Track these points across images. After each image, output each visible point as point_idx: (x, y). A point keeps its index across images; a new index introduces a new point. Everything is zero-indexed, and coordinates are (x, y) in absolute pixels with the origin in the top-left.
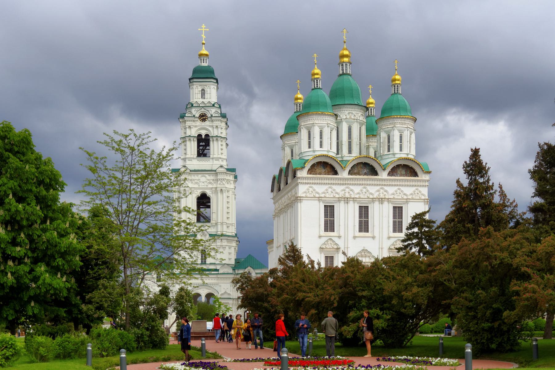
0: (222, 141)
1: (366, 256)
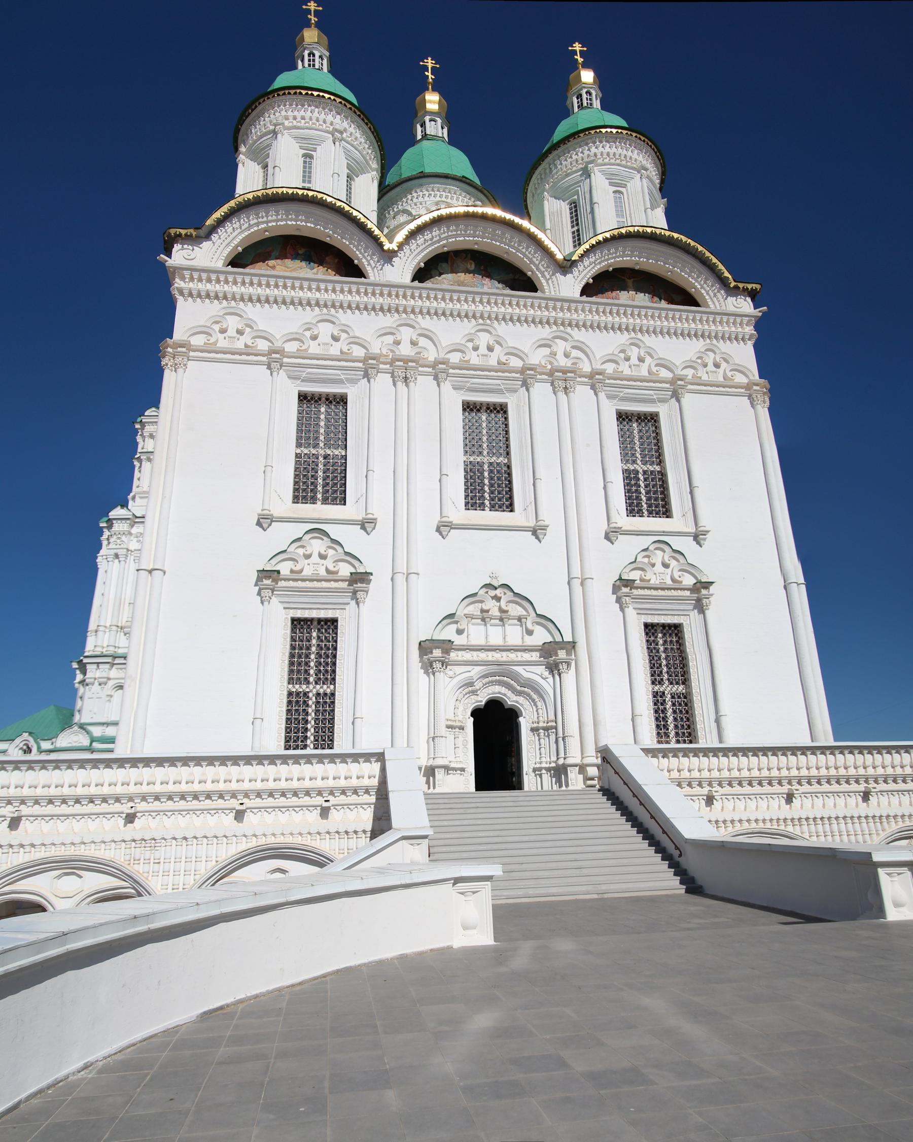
1: (503, 617)
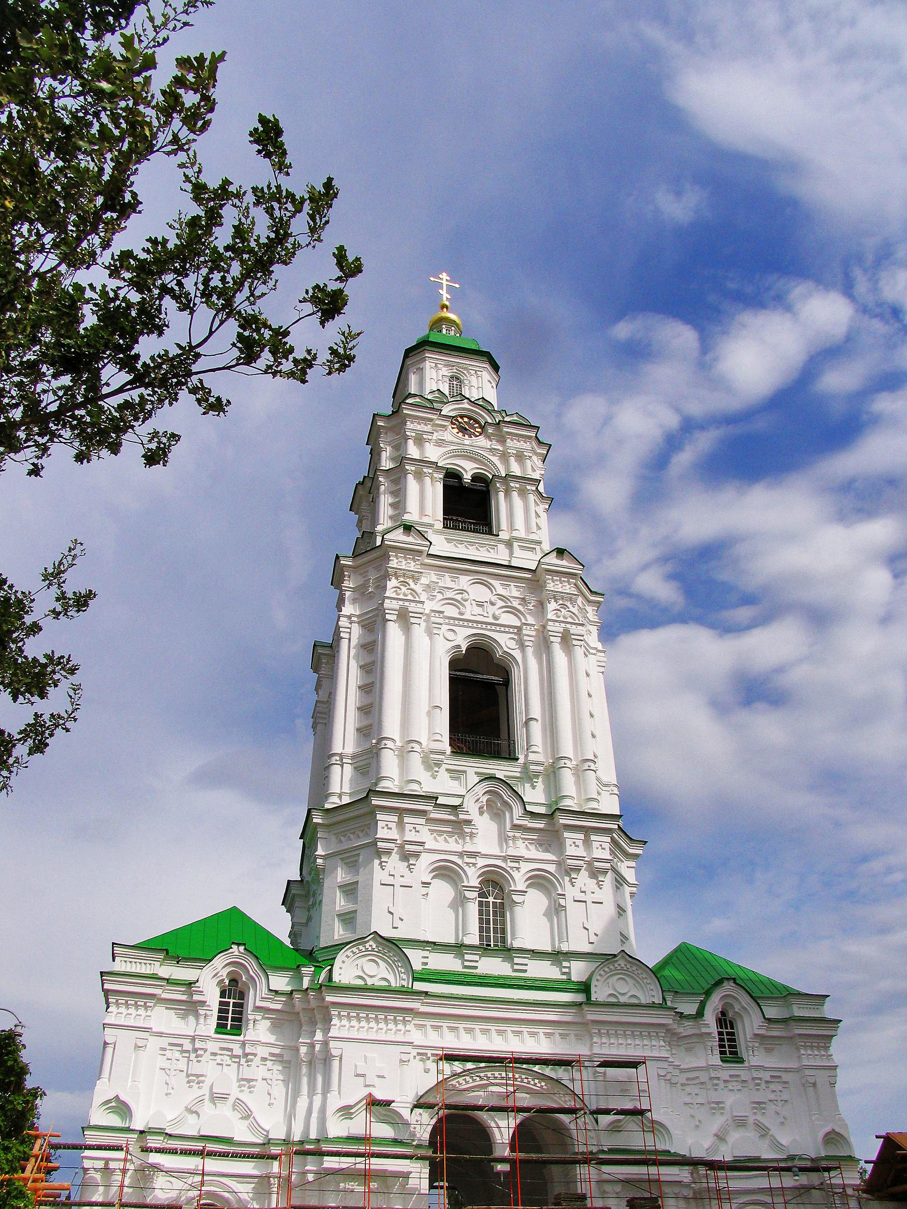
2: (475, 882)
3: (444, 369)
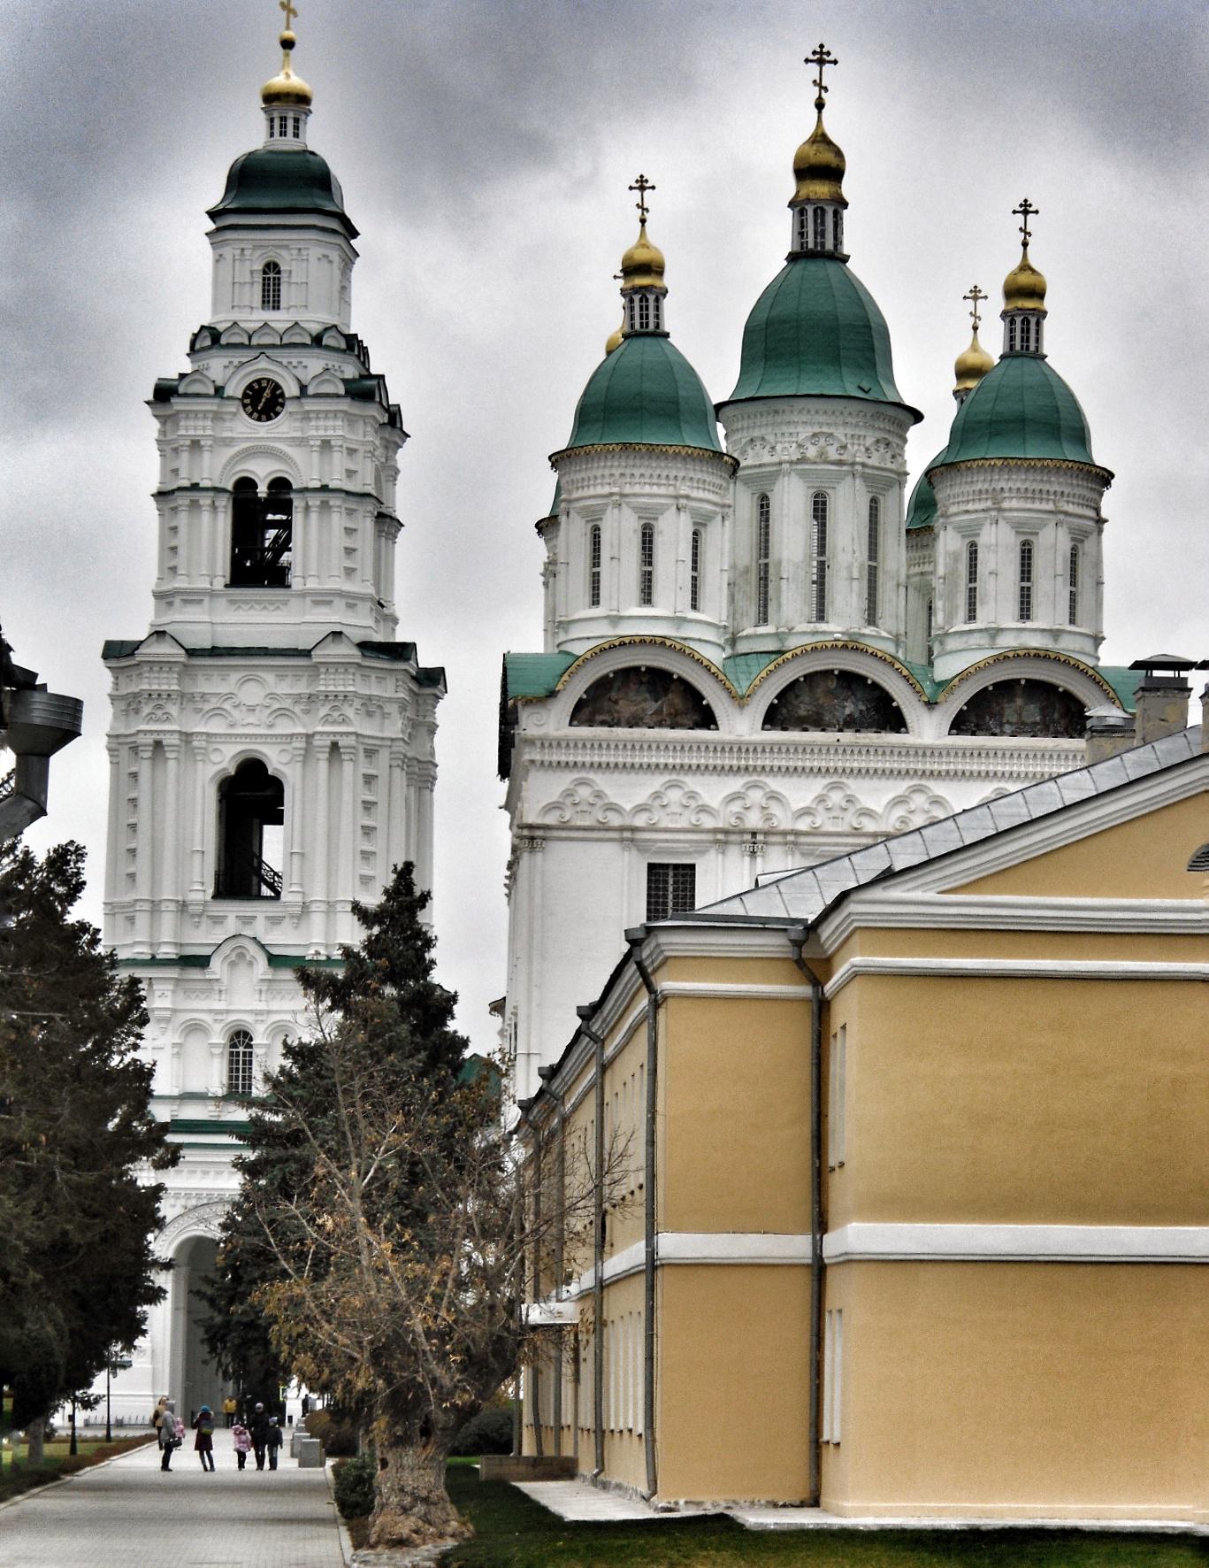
0: (350, 512)
2: (219, 1037)
3: (258, 253)
